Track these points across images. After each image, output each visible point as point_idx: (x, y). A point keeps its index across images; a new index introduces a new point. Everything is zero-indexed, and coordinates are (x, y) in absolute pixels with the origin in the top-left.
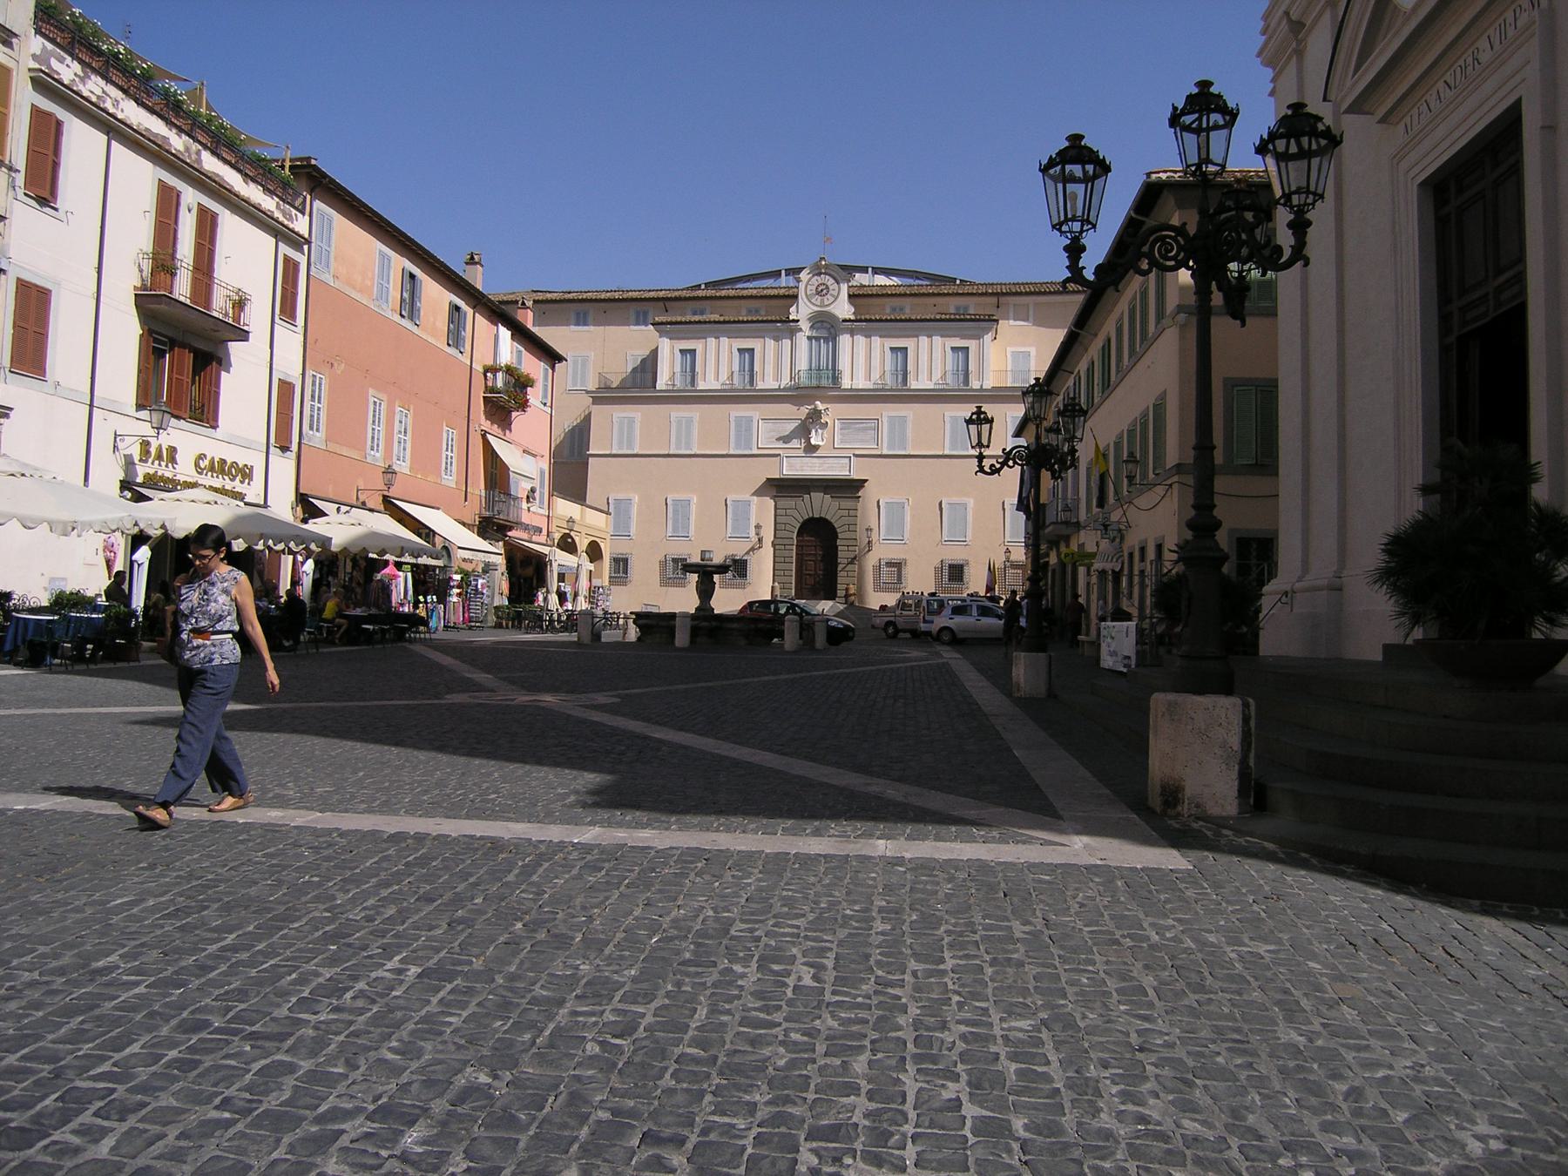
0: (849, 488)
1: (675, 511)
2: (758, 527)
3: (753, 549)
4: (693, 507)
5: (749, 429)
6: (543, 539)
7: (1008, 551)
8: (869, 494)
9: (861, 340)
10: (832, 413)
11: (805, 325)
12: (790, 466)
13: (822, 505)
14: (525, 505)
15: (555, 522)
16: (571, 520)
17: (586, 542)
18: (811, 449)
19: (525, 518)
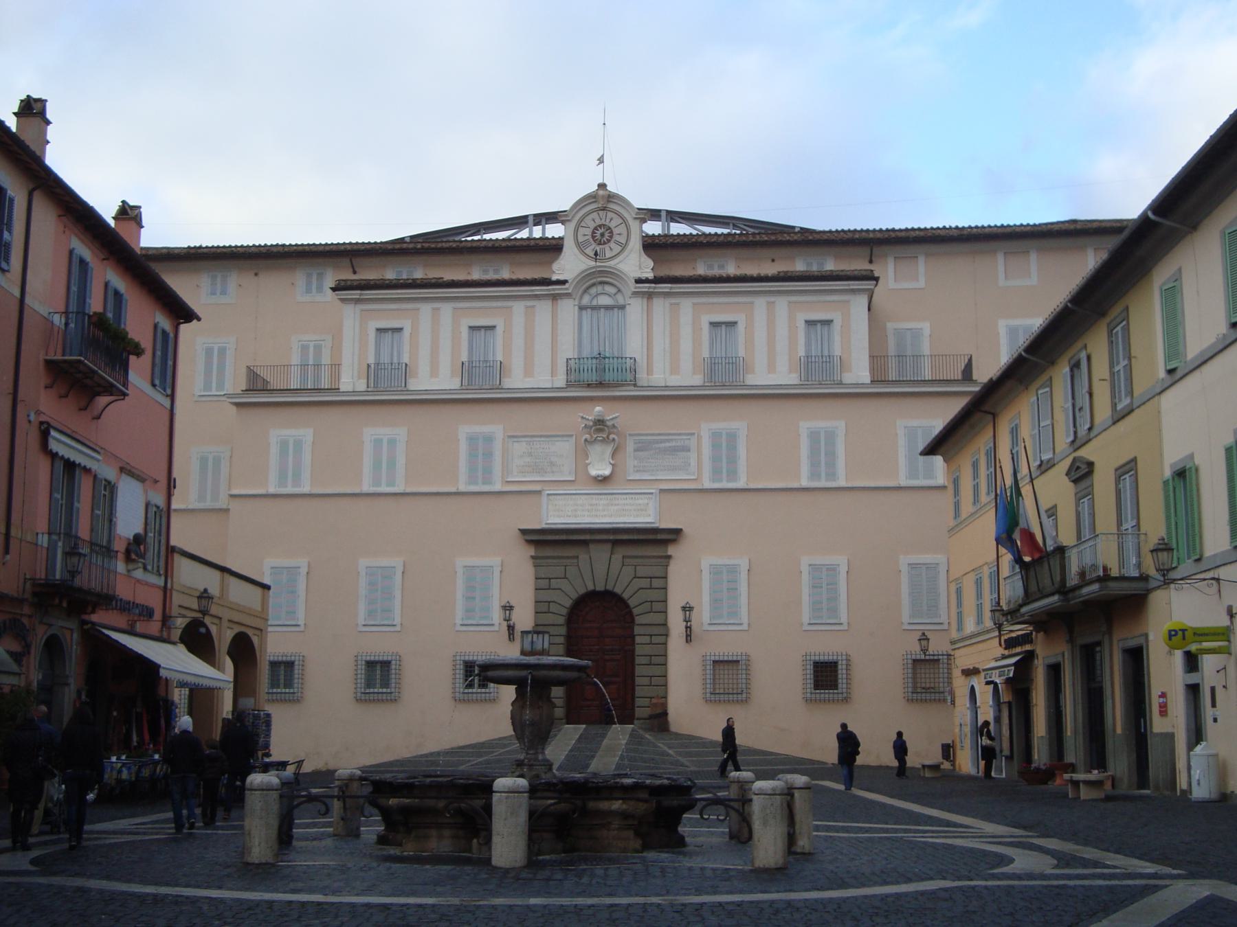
2: (508, 608)
5: (489, 455)
6: (154, 627)
7: (924, 638)
14: (121, 567)
15: (177, 599)
16: (204, 596)
17: (229, 635)
19: (123, 591)
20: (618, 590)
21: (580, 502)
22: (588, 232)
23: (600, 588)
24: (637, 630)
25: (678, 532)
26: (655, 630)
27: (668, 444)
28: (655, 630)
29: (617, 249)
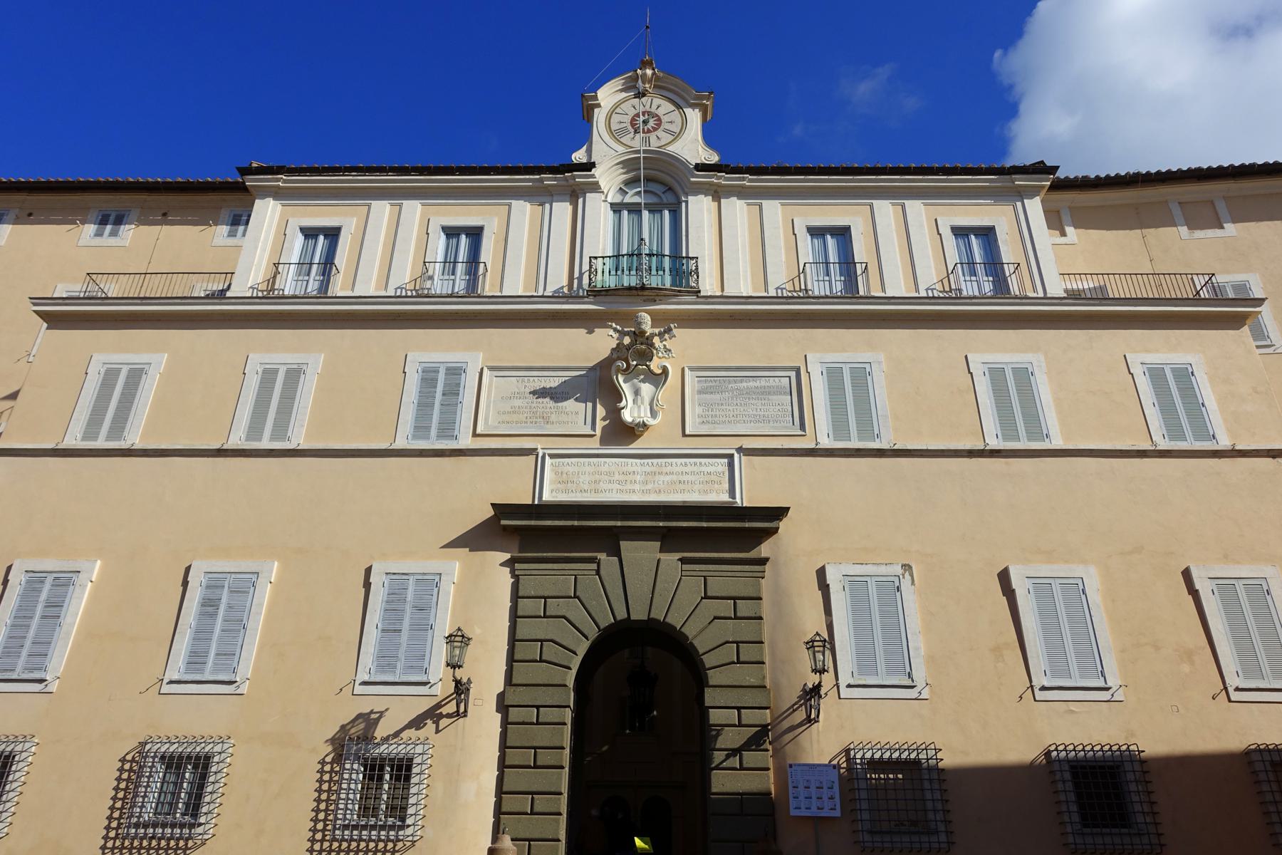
0: (731, 533)
1: (210, 605)
2: (458, 639)
3: (433, 714)
4: (264, 595)
5: (453, 391)
8: (791, 548)
9: (736, 209)
10: (681, 350)
11: (608, 177)
12: (563, 480)
13: (654, 582)
18: (621, 433)
20: (675, 620)
21: (605, 469)
22: (627, 119)
23: (639, 614)
24: (710, 697)
25: (779, 513)
26: (748, 698)
27: (752, 384)
28: (748, 698)
29: (666, 138)
